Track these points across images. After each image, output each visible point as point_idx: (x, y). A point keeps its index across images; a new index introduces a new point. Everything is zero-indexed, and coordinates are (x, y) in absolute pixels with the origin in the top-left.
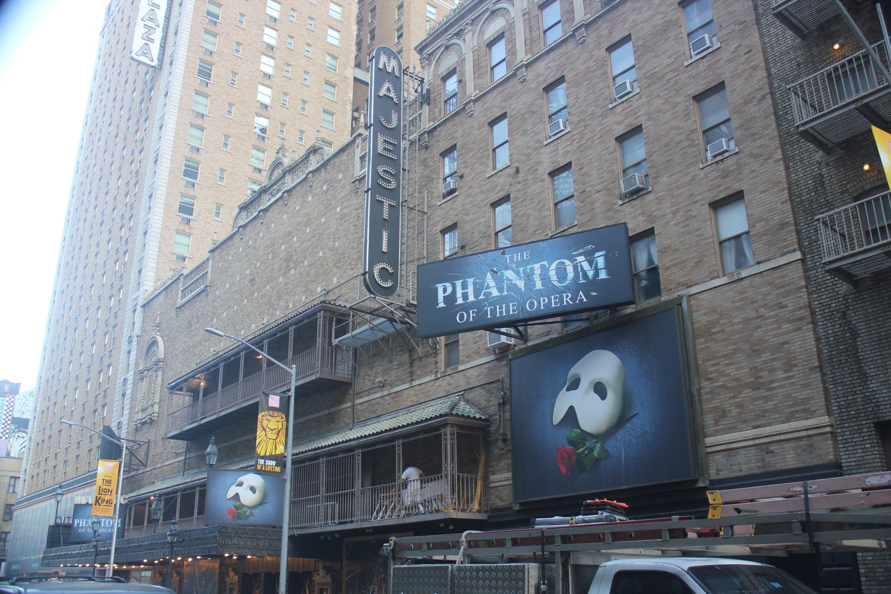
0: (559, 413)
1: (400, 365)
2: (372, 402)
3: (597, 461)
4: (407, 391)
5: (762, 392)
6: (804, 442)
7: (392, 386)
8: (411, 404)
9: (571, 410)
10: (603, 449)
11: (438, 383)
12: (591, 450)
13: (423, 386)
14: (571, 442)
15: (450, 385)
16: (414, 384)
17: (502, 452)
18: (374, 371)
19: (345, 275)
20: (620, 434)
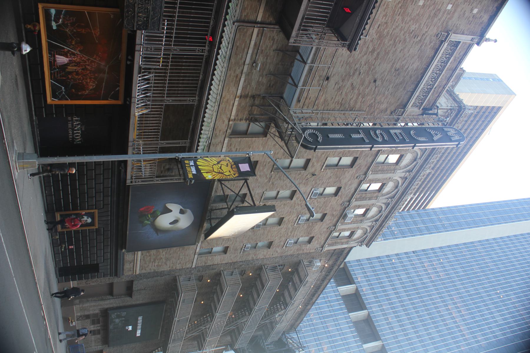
0: (170, 206)
1: (259, 83)
2: (246, 50)
3: (142, 222)
4: (235, 92)
5: (152, 260)
6: (132, 269)
7: (248, 74)
8: (223, 96)
9: (171, 211)
10: (147, 224)
11: (226, 122)
12: (148, 220)
13: (231, 107)
14: (154, 212)
15: (220, 131)
16: (237, 99)
17: (162, 168)
18: (272, 53)
19: (384, 13)
20: (152, 230)
